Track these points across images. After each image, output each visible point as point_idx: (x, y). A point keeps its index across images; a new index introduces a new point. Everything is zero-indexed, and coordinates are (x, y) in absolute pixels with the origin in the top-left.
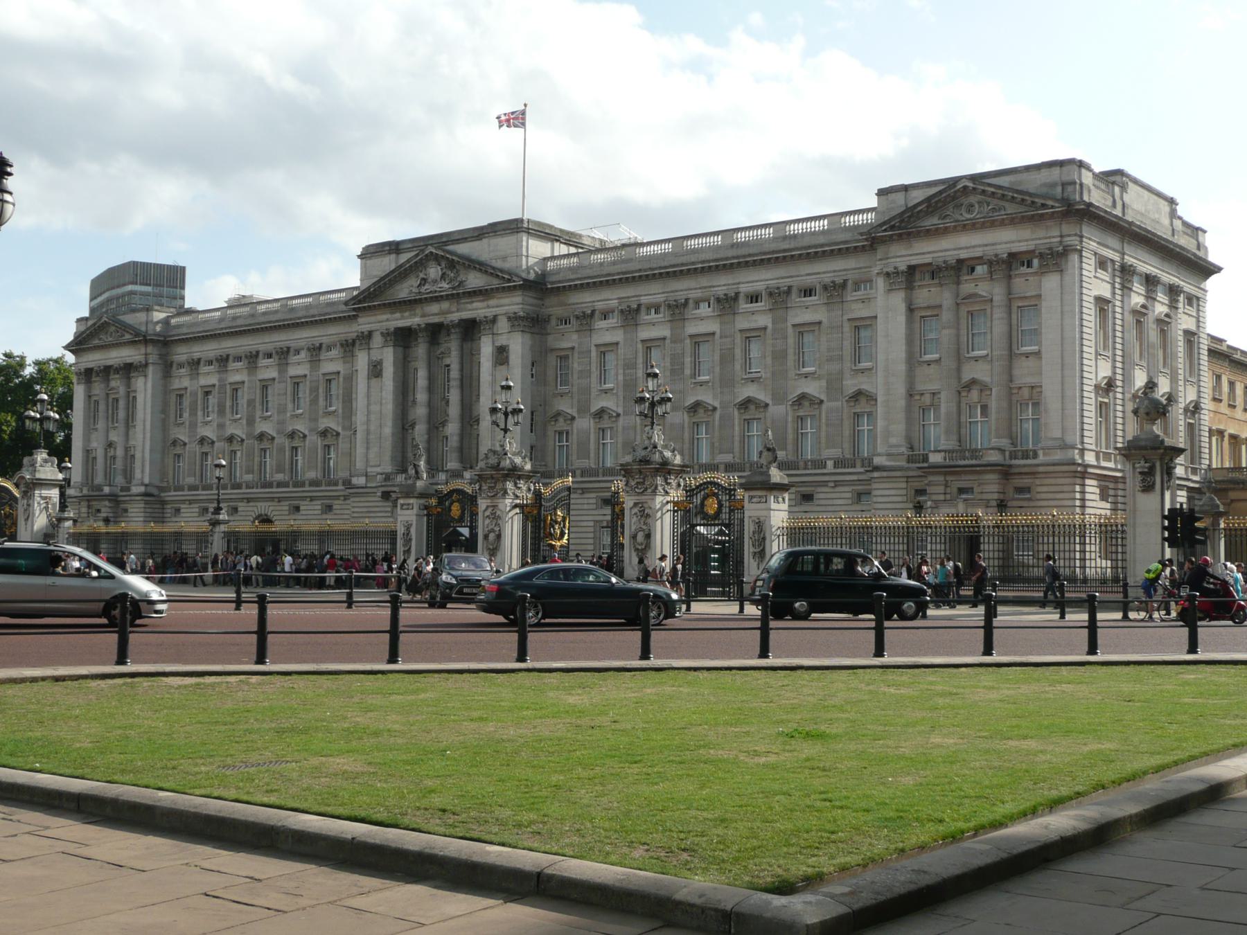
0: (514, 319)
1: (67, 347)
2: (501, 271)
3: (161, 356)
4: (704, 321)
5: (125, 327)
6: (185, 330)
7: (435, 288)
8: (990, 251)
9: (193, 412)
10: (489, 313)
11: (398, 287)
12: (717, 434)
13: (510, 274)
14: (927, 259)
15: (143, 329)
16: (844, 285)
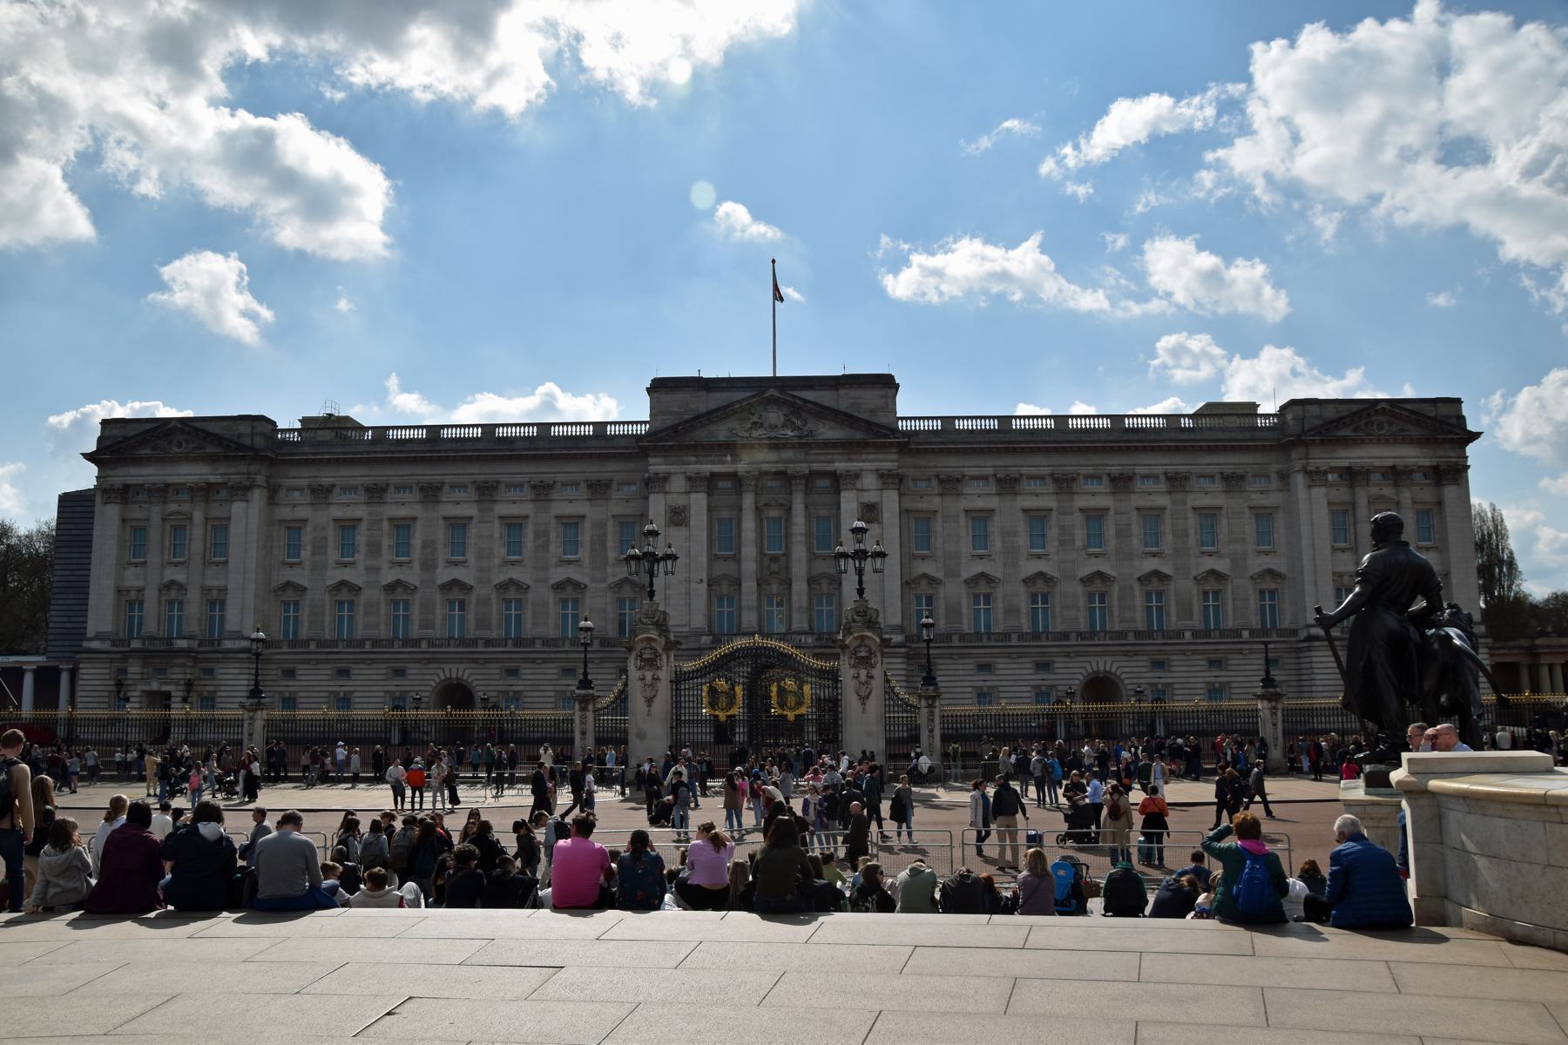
0: (883, 476)
1: (89, 457)
2: (878, 425)
3: (268, 477)
4: (1096, 496)
5: (218, 439)
6: (307, 449)
7: (772, 434)
8: (1399, 462)
9: (319, 547)
10: (854, 466)
11: (713, 428)
12: (1116, 603)
13: (895, 431)
14: (1345, 463)
15: (247, 442)
16: (1242, 477)
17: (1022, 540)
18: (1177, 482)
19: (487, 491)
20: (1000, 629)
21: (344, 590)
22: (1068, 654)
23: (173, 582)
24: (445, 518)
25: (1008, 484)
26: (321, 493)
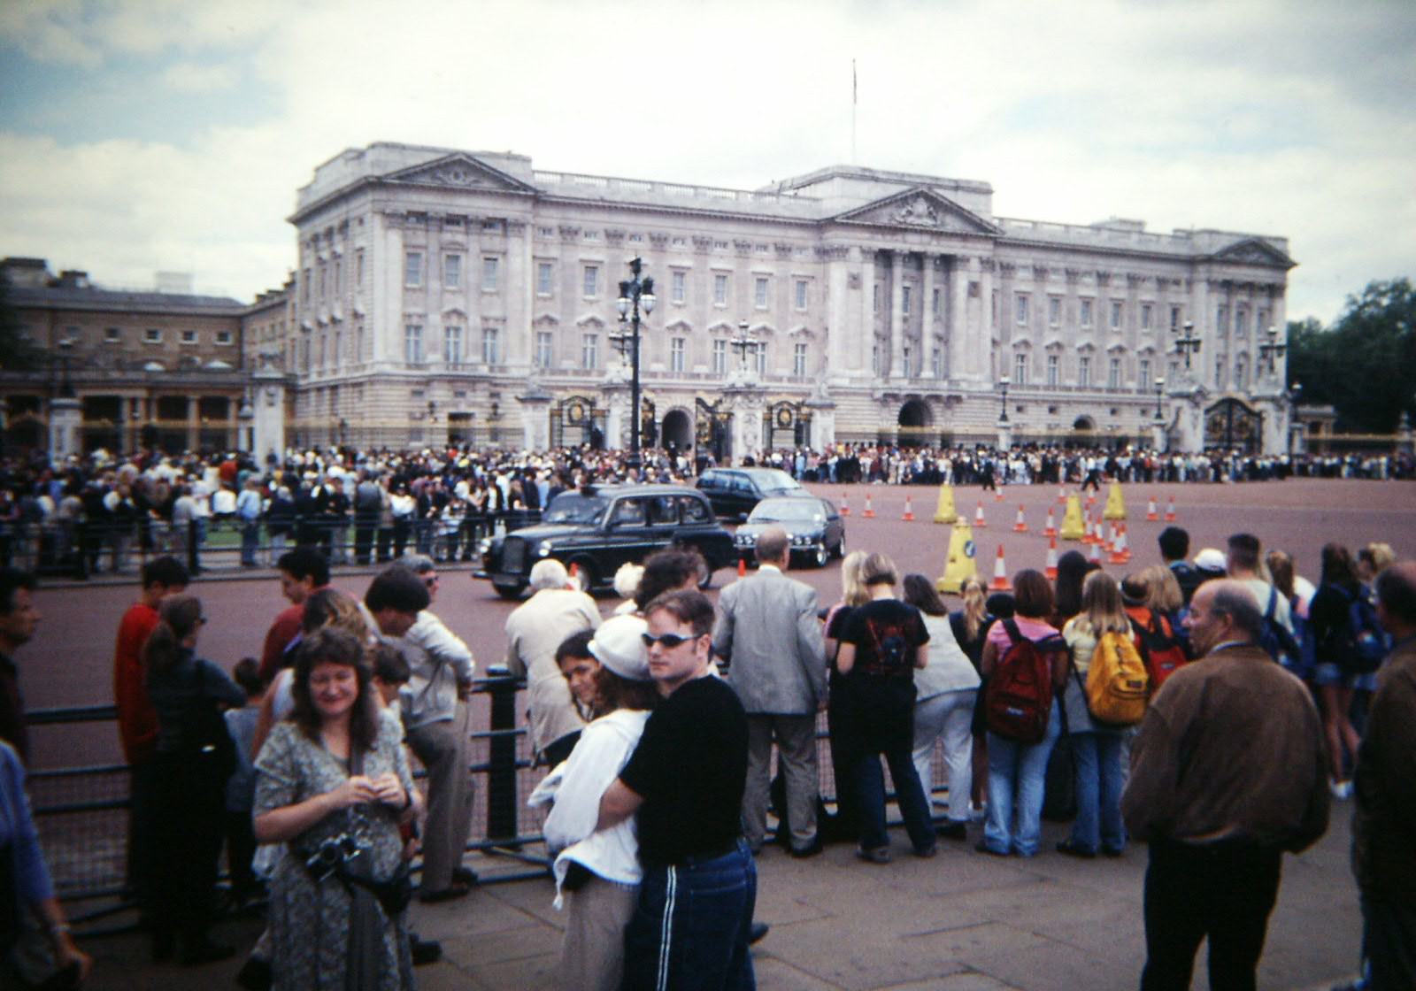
4: (1088, 288)
7: (919, 222)
9: (568, 287)
11: (878, 212)
13: (994, 230)
14: (1228, 277)
17: (1046, 316)
18: (1133, 280)
19: (702, 244)
20: (1031, 383)
21: (591, 325)
22: (1068, 402)
23: (457, 312)
24: (671, 267)
25: (1040, 273)
26: (568, 233)
